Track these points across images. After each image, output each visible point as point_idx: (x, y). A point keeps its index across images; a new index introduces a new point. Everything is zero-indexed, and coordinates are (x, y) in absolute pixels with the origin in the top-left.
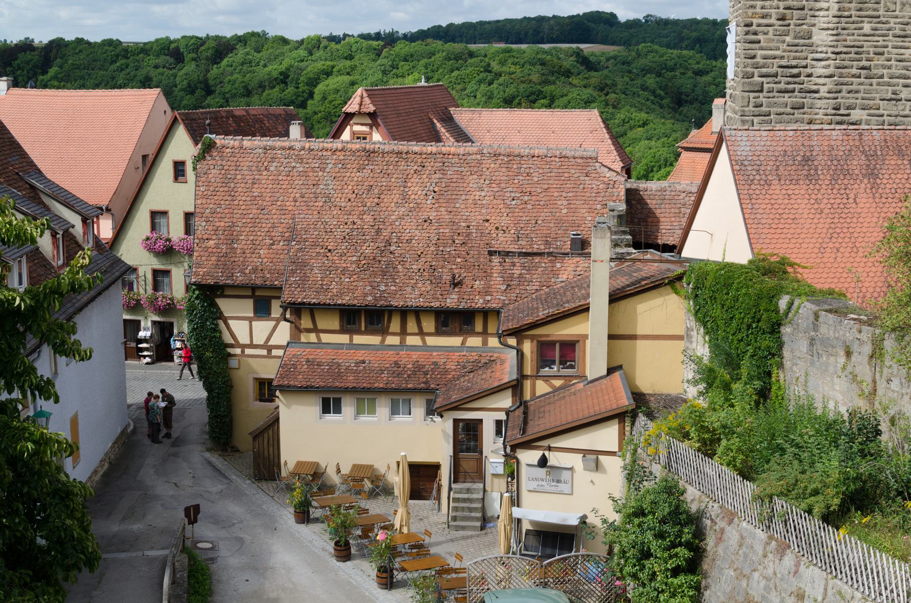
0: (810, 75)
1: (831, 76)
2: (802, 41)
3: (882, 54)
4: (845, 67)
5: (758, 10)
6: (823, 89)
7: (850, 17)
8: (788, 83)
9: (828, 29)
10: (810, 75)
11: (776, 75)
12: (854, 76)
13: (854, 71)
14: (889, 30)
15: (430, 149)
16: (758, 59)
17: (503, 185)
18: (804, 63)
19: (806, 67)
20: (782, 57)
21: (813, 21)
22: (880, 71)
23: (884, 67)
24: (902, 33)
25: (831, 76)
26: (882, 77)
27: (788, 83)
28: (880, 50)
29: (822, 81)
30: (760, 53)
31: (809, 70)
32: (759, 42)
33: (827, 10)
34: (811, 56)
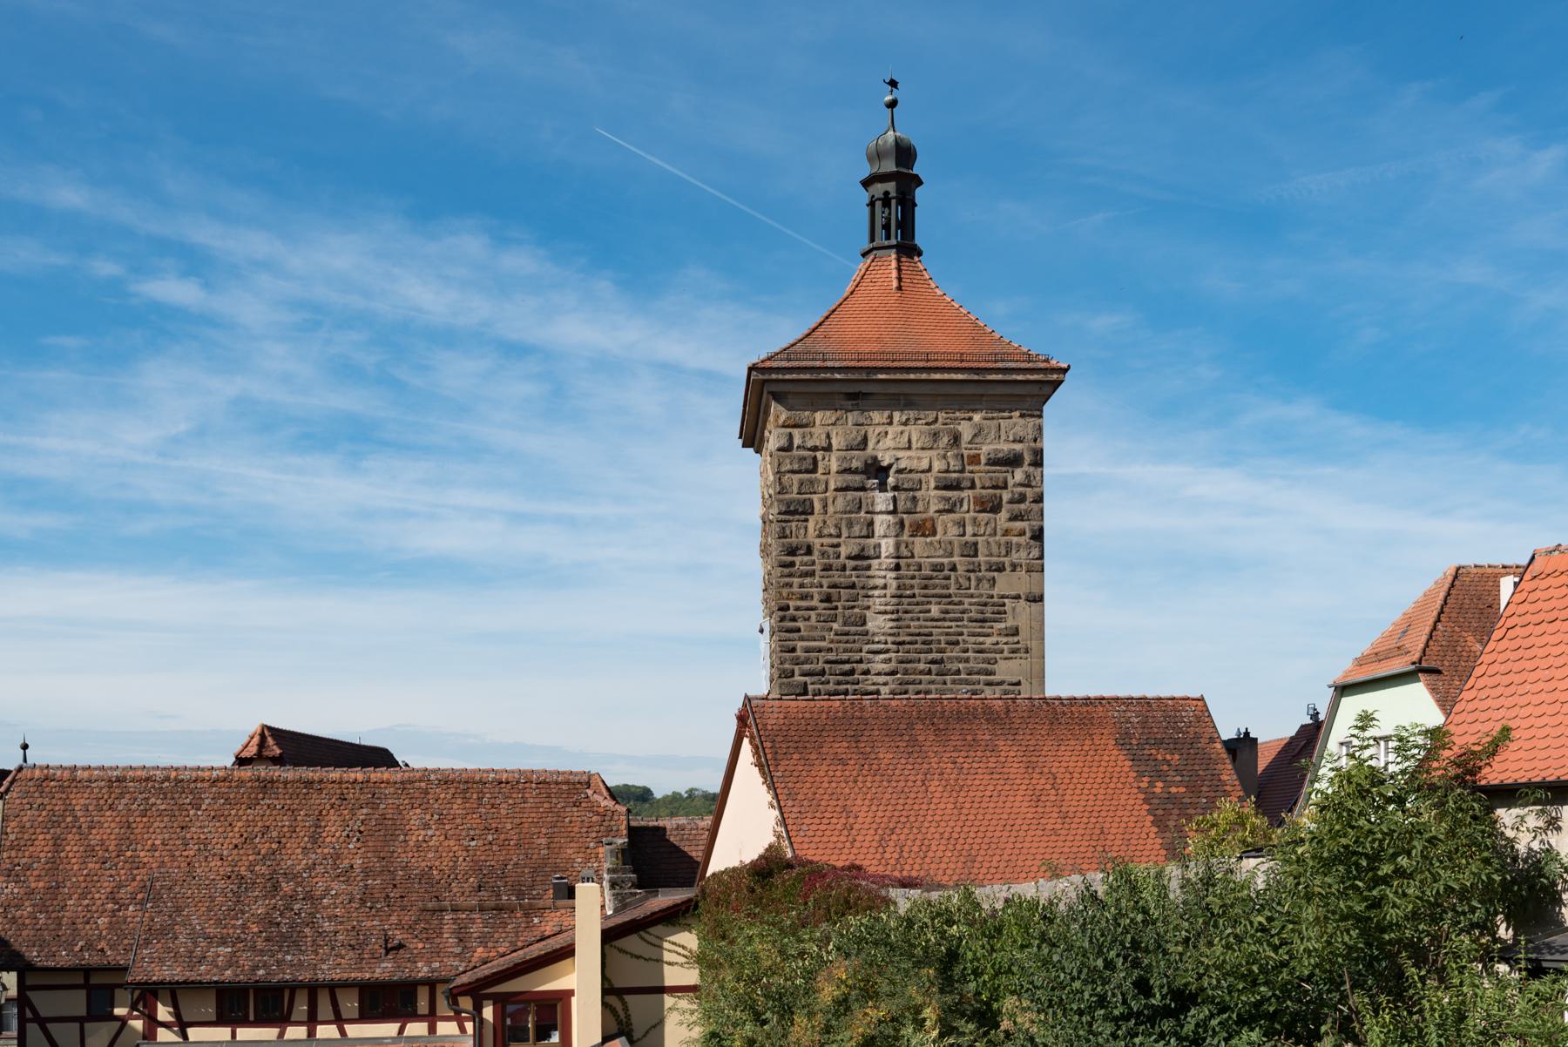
0: (867, 672)
1: (893, 673)
2: (853, 629)
3: (957, 643)
4: (910, 662)
5: (795, 589)
6: (884, 690)
7: (914, 596)
8: (839, 683)
9: (885, 613)
10: (867, 672)
11: (823, 673)
12: (921, 673)
13: (922, 666)
14: (963, 612)
15: (353, 776)
16: (799, 653)
17: (458, 821)
18: (857, 656)
19: (861, 661)
20: (830, 650)
21: (866, 602)
22: (954, 666)
23: (960, 660)
24: (980, 616)
25: (893, 673)
26: (958, 672)
27: (839, 683)
28: (954, 638)
29: (882, 679)
30: (800, 644)
31: (863, 666)
32: (799, 630)
33: (885, 587)
34: (866, 648)
